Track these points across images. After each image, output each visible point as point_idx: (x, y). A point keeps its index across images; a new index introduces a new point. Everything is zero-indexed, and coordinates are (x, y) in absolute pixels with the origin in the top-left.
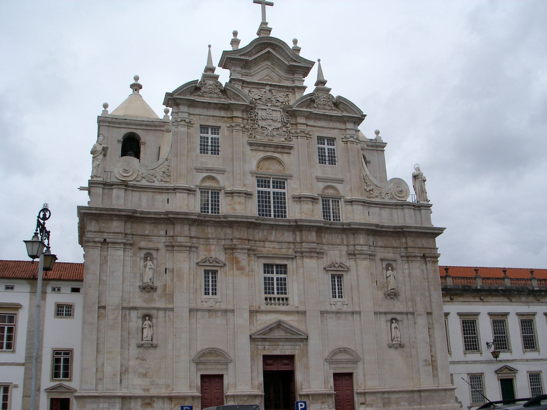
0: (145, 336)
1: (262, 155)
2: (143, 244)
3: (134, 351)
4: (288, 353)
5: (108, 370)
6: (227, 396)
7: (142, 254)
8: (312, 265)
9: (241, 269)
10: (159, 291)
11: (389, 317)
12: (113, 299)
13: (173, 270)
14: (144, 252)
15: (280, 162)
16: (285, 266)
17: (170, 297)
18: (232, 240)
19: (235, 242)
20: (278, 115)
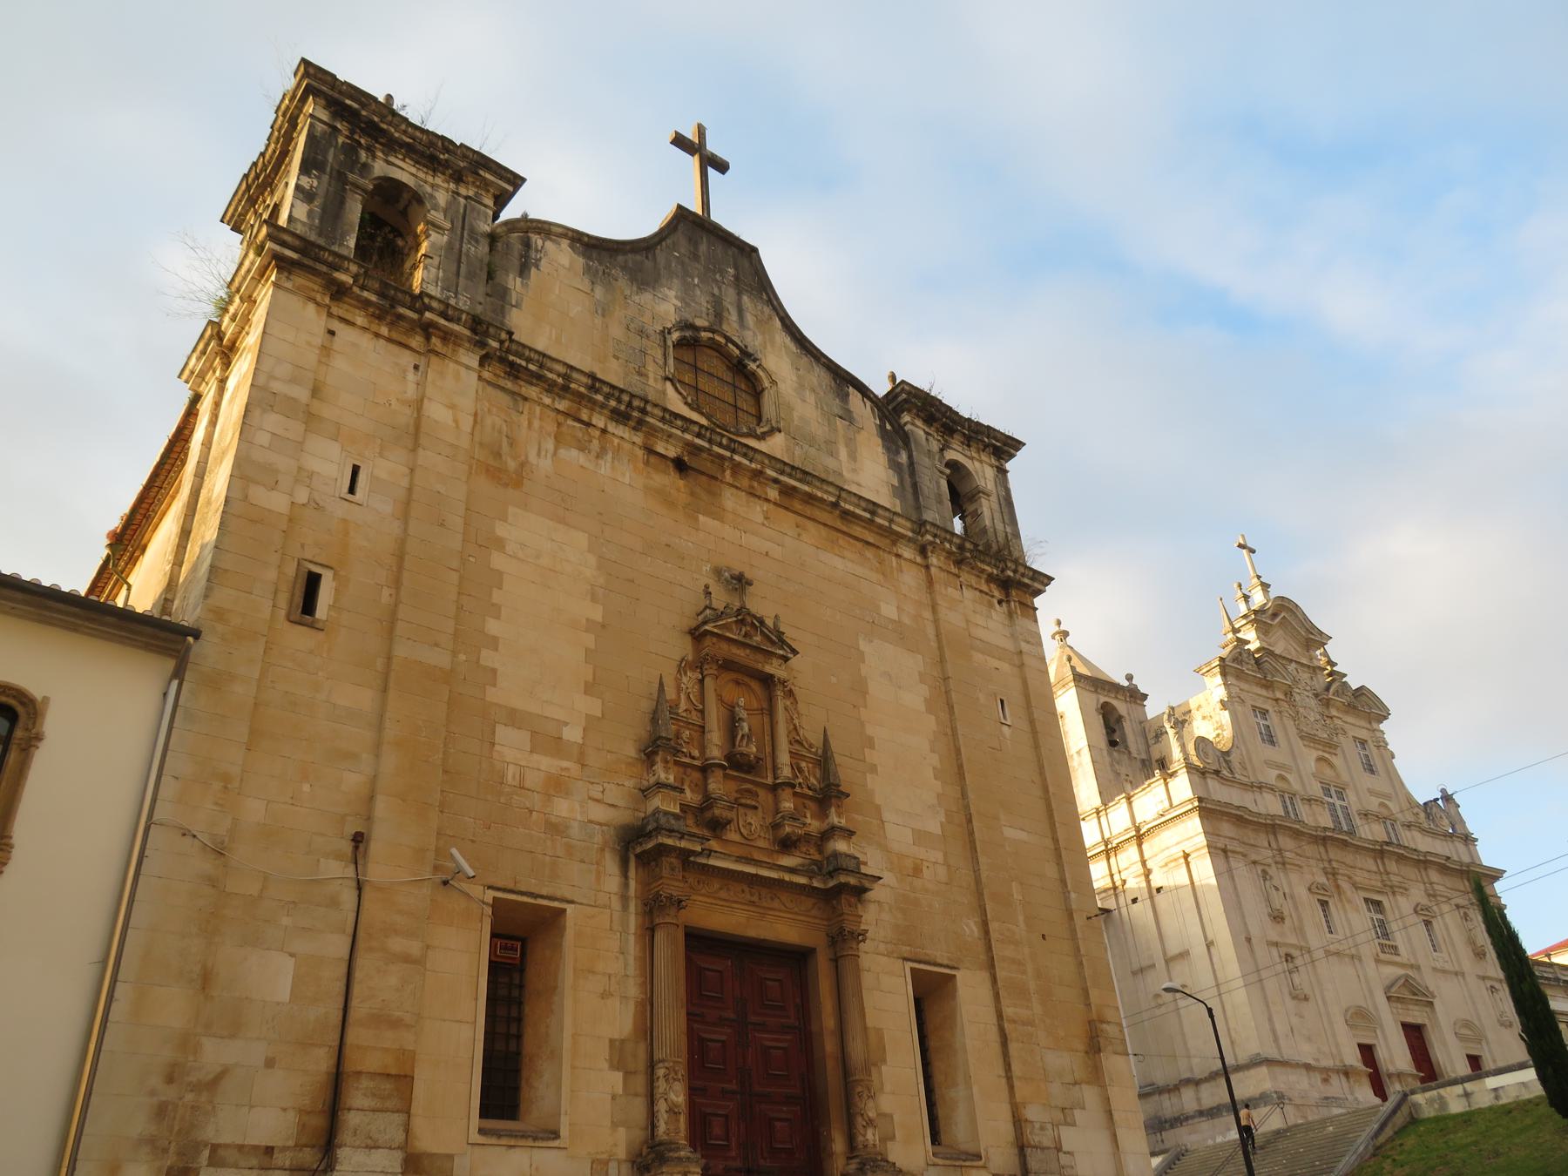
0: (1297, 980)
1: (1315, 754)
2: (1254, 857)
3: (1290, 1003)
4: (1419, 1021)
5: (1278, 1027)
6: (1390, 1076)
7: (1259, 868)
8: (1405, 904)
9: (1349, 901)
10: (1287, 920)
11: (1489, 983)
12: (1255, 932)
13: (1292, 897)
14: (1259, 868)
15: (1331, 765)
16: (1378, 904)
17: (1300, 931)
18: (1330, 861)
19: (1335, 865)
20: (1313, 702)
